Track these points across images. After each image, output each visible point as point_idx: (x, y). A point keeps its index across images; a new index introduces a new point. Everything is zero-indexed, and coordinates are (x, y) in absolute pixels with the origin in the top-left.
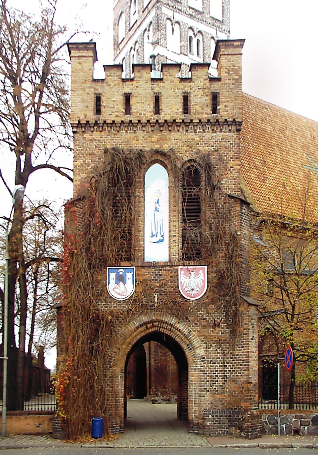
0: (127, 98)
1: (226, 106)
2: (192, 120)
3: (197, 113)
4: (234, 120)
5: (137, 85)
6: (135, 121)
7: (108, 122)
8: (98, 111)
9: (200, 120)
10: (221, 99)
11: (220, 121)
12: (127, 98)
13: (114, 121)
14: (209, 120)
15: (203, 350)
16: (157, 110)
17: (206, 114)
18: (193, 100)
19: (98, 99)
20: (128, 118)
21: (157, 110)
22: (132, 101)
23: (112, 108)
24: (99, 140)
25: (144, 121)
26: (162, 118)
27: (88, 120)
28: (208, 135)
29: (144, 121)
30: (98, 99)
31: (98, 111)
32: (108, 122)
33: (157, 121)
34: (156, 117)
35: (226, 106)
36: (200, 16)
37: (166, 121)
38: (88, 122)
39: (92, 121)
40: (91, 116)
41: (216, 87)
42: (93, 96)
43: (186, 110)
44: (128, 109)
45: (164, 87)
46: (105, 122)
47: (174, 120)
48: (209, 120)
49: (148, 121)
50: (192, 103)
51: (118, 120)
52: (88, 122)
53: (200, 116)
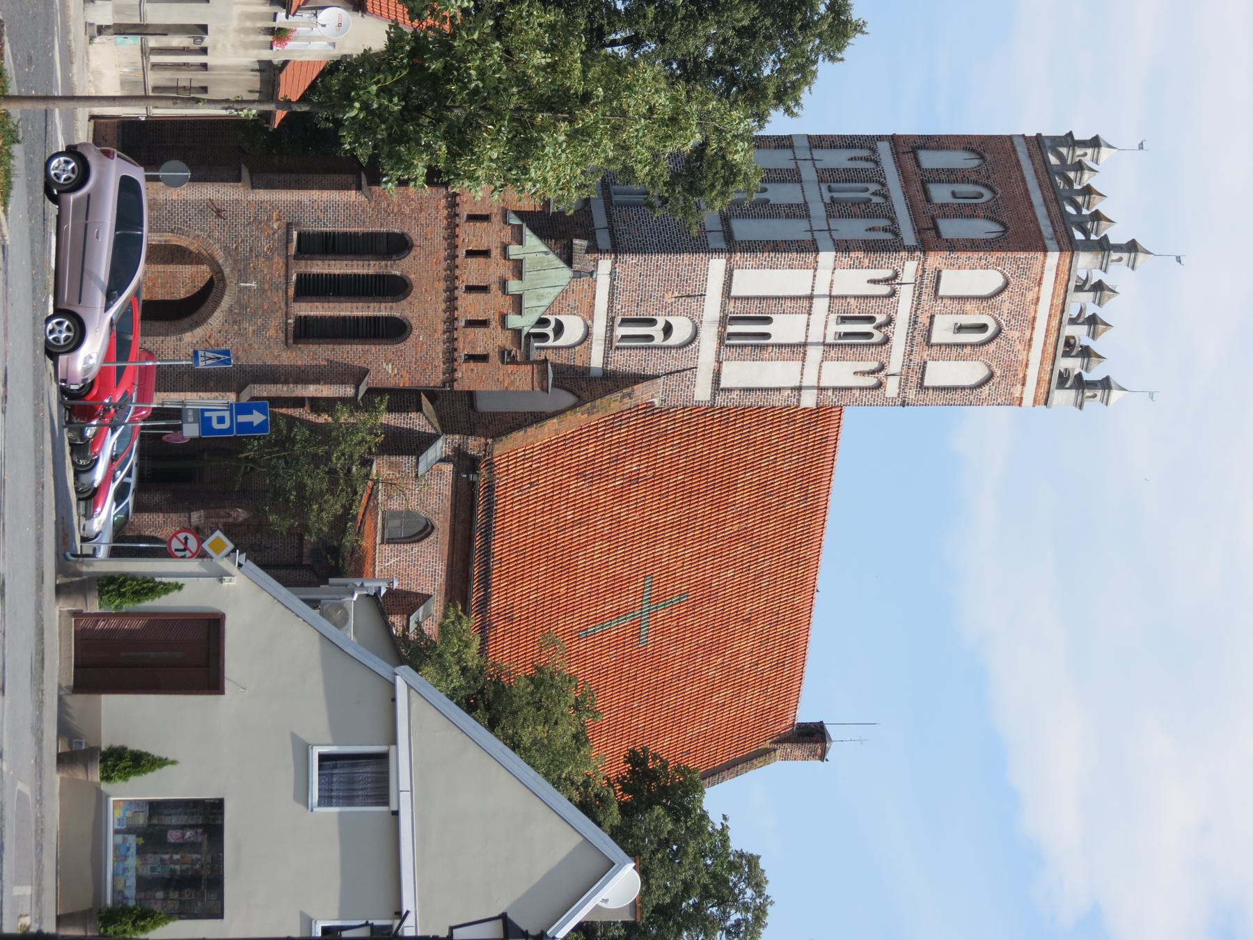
0: (485, 253)
1: (472, 370)
2: (456, 329)
3: (465, 336)
4: (456, 380)
5: (500, 265)
6: (458, 261)
7: (457, 228)
8: (473, 218)
9: (456, 339)
10: (481, 365)
11: (456, 363)
12: (485, 253)
13: (457, 236)
14: (456, 350)
15: (190, 339)
16: (470, 289)
17: (464, 349)
18: (479, 332)
19: (485, 218)
20: (461, 252)
21: (470, 289)
22: (482, 260)
23: (474, 233)
24: (437, 217)
25: (457, 272)
26: (460, 293)
27: (460, 206)
28: (440, 348)
29: (457, 272)
30: (485, 218)
31: (473, 218)
32: (457, 229)
33: (457, 288)
34: (462, 286)
35: (472, 370)
36: (919, 339)
37: (457, 298)
38: (458, 205)
39: (458, 210)
40: (465, 211)
41: (494, 358)
42: (489, 212)
43: (471, 323)
44: (470, 253)
45: (496, 296)
46: (457, 226)
47: (457, 309)
48: (456, 350)
49: (457, 277)
50: (477, 330)
51: (459, 241)
52: (458, 205)
53: (461, 339)
